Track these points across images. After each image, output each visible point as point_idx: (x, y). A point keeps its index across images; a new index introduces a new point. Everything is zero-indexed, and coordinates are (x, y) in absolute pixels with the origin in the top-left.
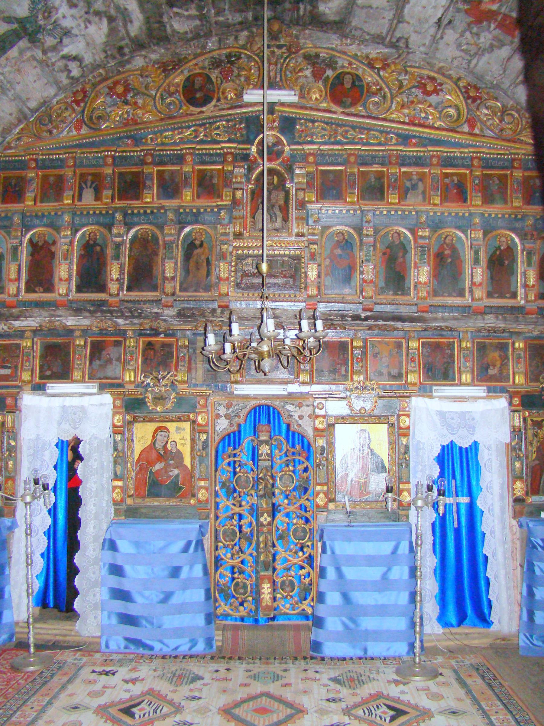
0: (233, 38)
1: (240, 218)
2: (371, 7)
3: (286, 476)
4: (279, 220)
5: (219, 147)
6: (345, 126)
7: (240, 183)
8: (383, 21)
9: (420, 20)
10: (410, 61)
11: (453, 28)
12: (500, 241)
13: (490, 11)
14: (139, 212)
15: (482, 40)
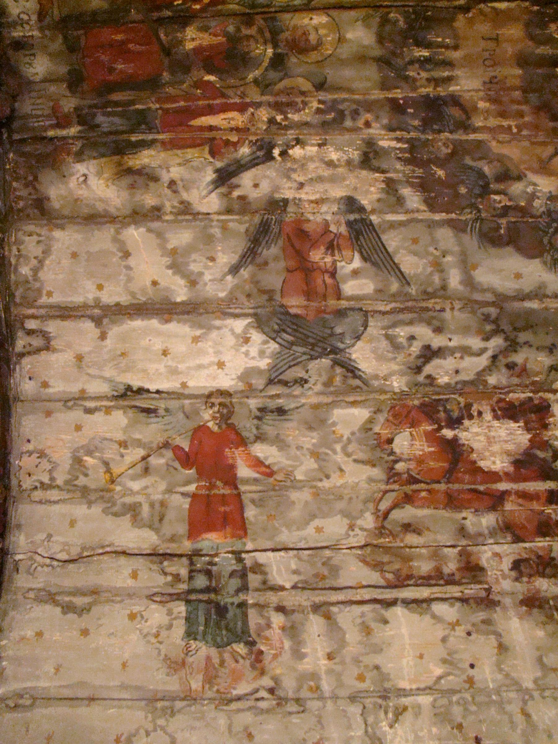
2: (127, 255)
8: (93, 288)
9: (123, 354)
11: (132, 424)
13: (232, 467)
15: (136, 486)
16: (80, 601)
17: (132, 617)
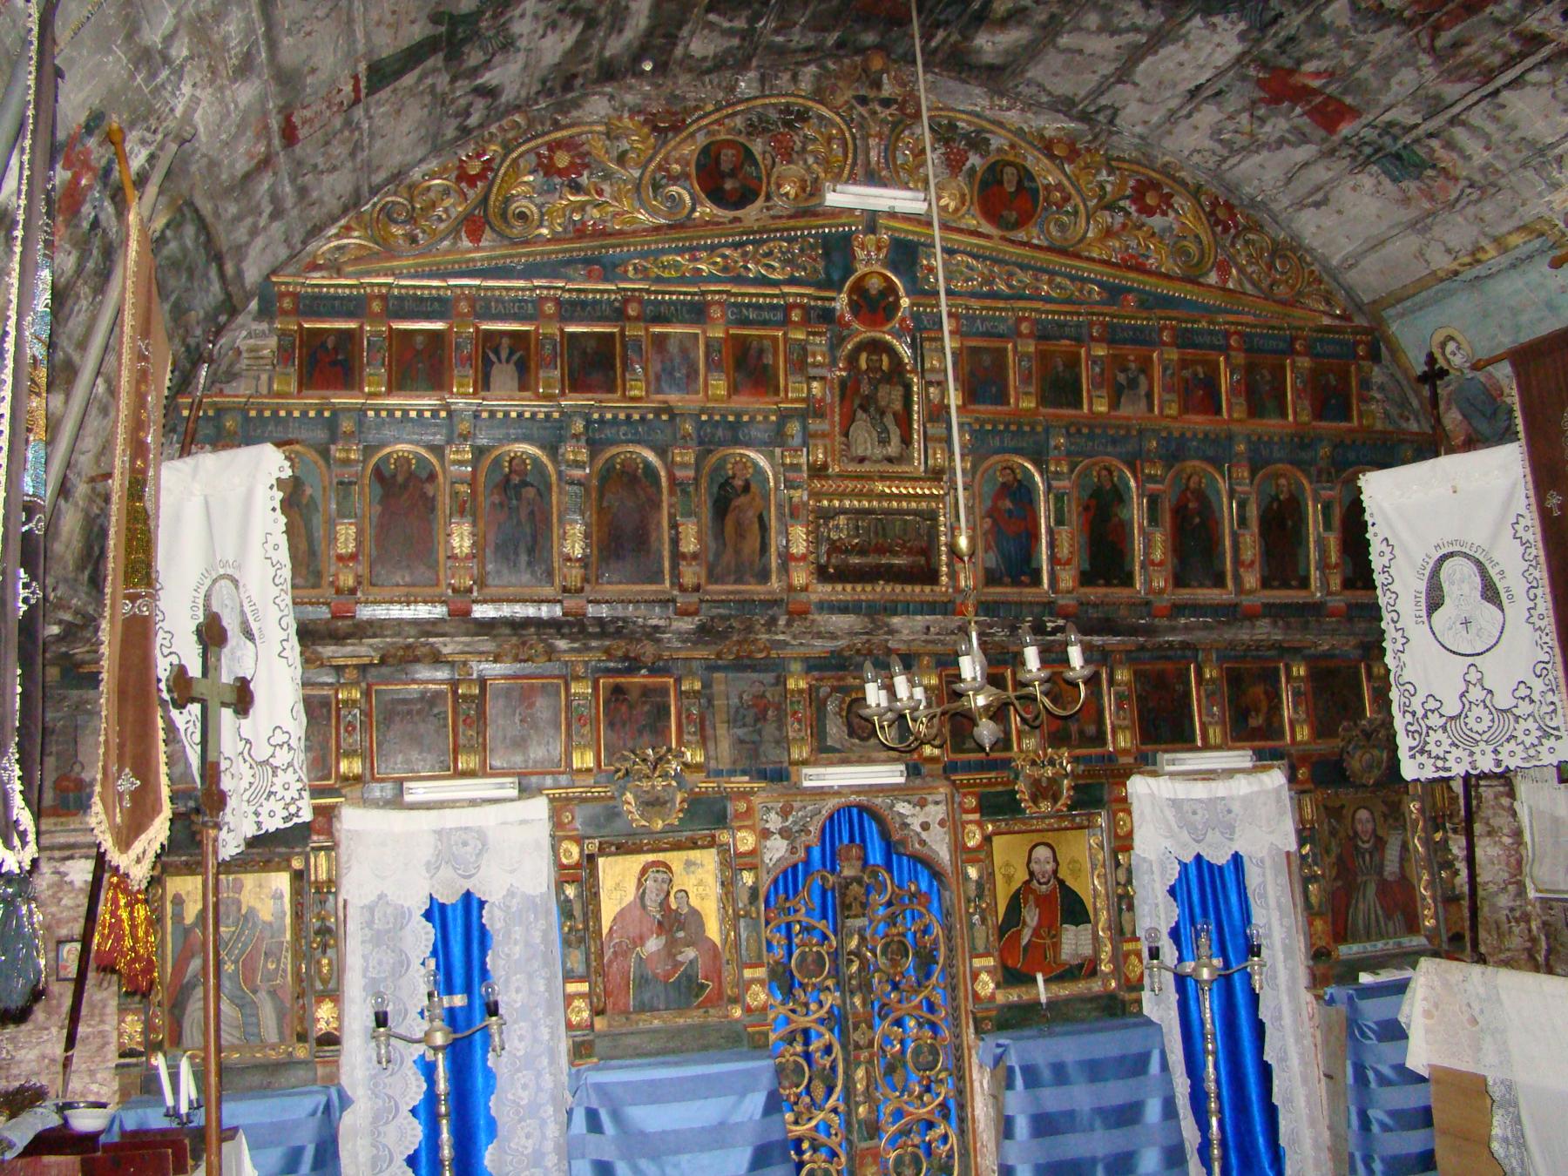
0: (787, 76)
1: (824, 435)
3: (894, 946)
4: (895, 439)
5: (777, 292)
6: (1007, 263)
7: (820, 365)
10: (1113, 147)
11: (1219, 105)
12: (1278, 486)
13: (1305, 87)
14: (615, 417)
15: (1268, 128)
16: (1318, 197)
17: (1354, 189)
